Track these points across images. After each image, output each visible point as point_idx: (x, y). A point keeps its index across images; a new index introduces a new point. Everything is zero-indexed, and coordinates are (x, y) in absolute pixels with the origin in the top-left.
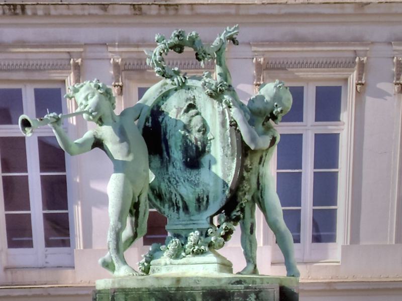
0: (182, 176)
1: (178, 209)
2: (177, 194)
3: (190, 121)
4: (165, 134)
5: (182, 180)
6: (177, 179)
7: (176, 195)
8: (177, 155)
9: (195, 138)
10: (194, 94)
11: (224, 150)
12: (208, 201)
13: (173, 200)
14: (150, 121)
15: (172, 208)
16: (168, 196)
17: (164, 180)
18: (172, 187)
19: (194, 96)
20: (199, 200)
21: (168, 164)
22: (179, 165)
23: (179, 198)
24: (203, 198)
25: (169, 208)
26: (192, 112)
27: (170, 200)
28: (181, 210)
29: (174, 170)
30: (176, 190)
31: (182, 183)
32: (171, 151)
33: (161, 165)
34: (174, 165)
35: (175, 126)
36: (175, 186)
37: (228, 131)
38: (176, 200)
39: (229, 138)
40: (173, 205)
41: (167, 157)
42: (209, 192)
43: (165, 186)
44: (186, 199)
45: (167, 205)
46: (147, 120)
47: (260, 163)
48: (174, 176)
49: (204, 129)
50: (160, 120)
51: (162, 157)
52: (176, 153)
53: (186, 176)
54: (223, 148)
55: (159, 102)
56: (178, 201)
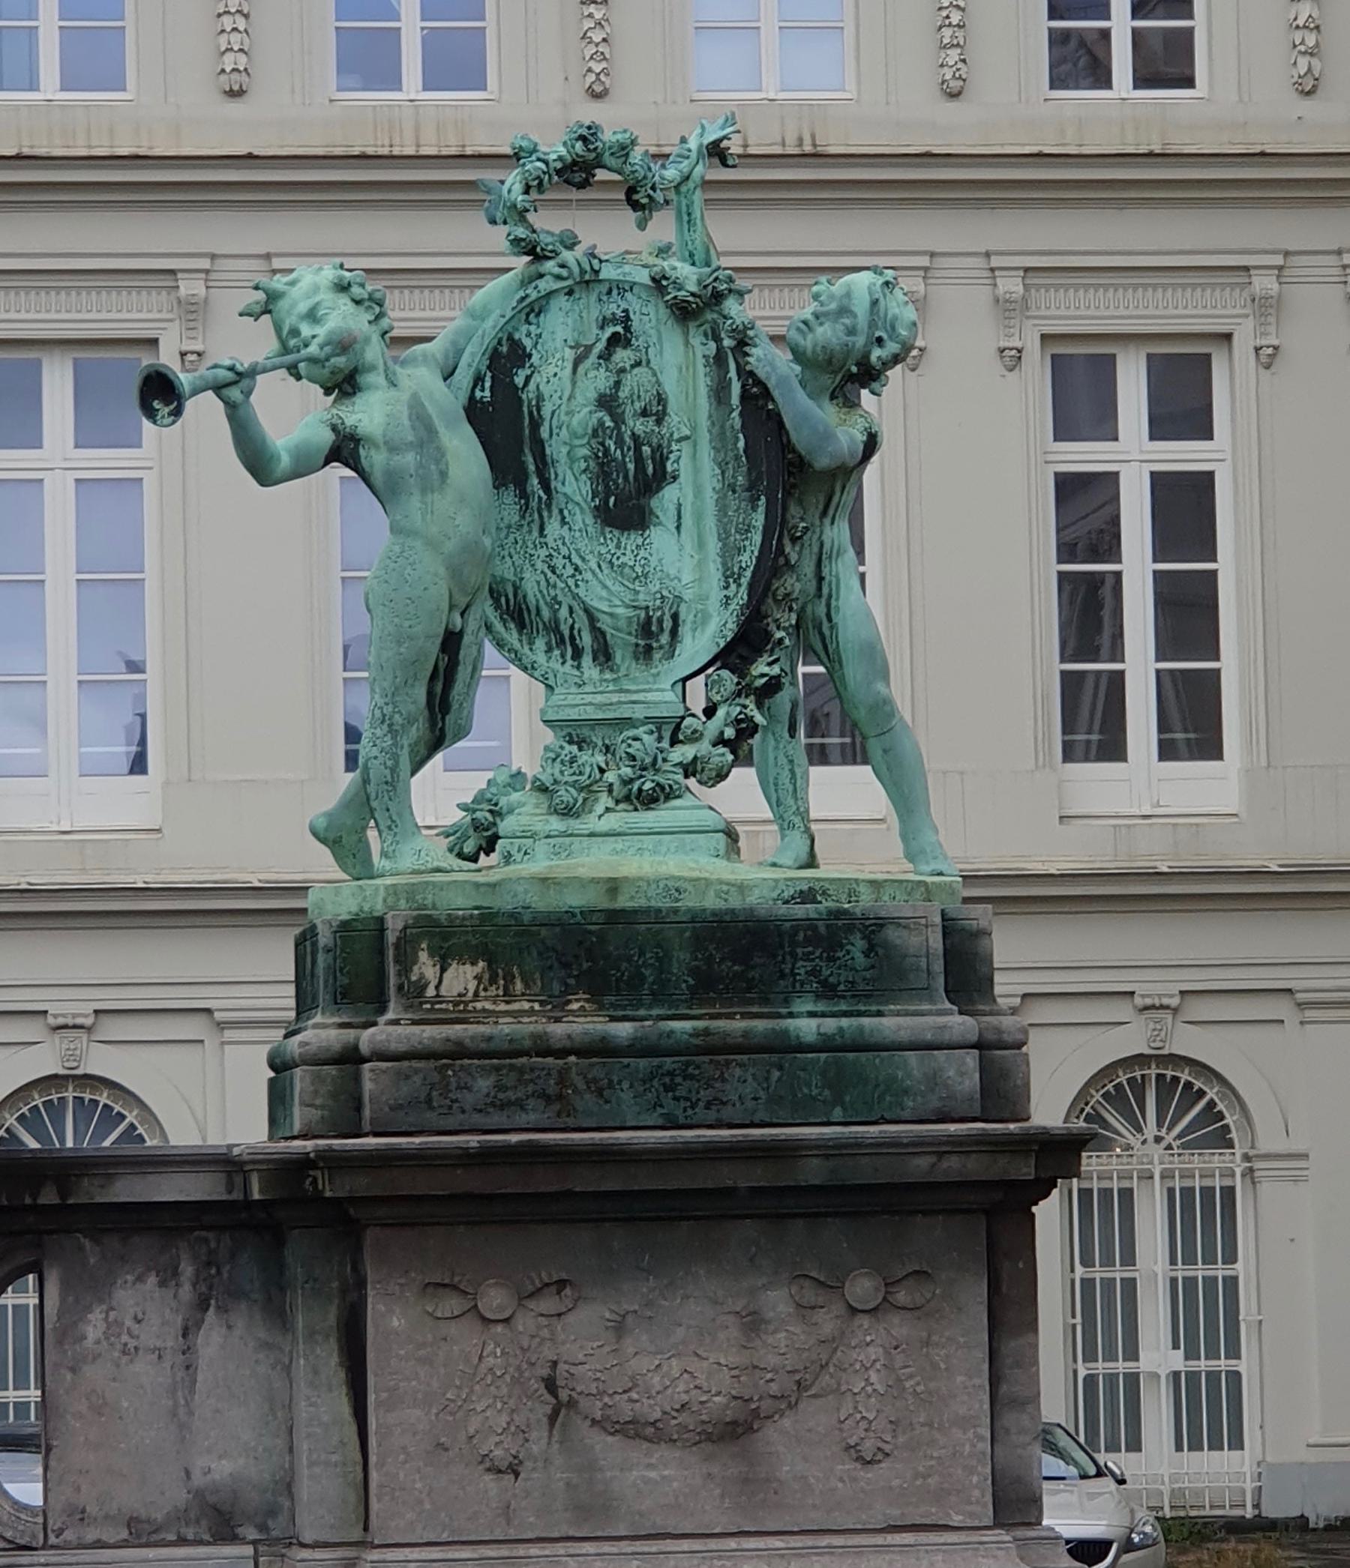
1: (577, 654)
2: (576, 608)
3: (618, 384)
4: (536, 424)
5: (595, 566)
6: (576, 560)
7: (571, 611)
8: (574, 486)
9: (633, 434)
10: (624, 305)
11: (723, 473)
12: (674, 632)
14: (488, 384)
15: (557, 652)
16: (546, 613)
19: (626, 311)
20: (647, 628)
21: (545, 514)
24: (660, 621)
25: (549, 650)
26: (622, 356)
27: (553, 628)
28: (587, 660)
33: (523, 517)
34: (563, 518)
35: (569, 399)
37: (735, 414)
38: (572, 628)
39: (741, 436)
40: (561, 642)
42: (679, 599)
43: (538, 583)
44: (605, 623)
45: (540, 644)
46: (478, 380)
47: (824, 513)
48: (564, 551)
49: (657, 410)
50: (519, 380)
51: (524, 494)
54: (722, 466)
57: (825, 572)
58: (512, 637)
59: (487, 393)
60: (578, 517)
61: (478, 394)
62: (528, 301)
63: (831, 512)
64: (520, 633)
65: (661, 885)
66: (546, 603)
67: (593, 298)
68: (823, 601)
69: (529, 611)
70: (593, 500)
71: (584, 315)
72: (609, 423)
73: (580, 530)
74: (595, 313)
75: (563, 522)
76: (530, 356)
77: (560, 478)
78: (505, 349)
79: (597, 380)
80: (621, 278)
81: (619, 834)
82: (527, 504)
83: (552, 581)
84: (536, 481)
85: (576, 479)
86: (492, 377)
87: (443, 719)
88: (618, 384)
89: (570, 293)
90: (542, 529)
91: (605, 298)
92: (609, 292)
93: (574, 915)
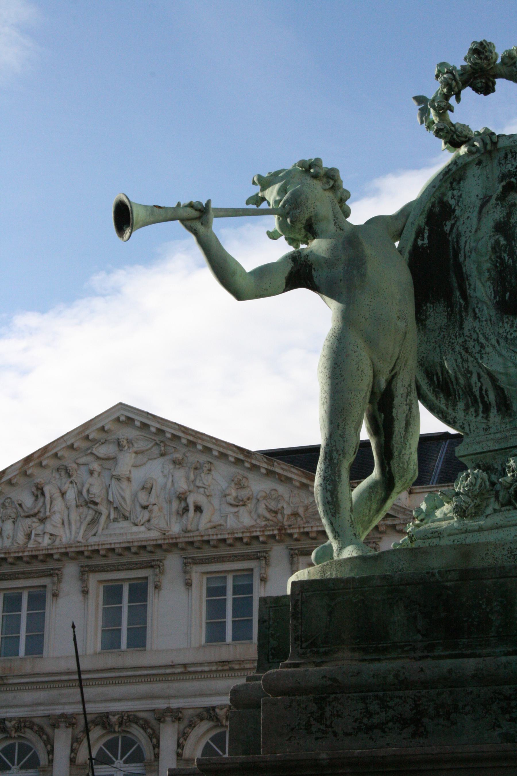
0: (493, 333)
1: (487, 409)
2: (482, 374)
3: (509, 215)
4: (456, 253)
5: (494, 342)
6: (482, 340)
7: (479, 377)
13: (474, 390)
14: (426, 235)
15: (472, 410)
16: (462, 381)
17: (453, 350)
18: (471, 359)
21: (464, 314)
22: (488, 311)
23: (487, 384)
25: (467, 409)
27: (469, 390)
28: (494, 411)
29: (476, 324)
30: (480, 366)
31: (494, 347)
32: (470, 285)
33: (449, 319)
34: (475, 314)
36: (478, 356)
38: (481, 389)
40: (475, 401)
41: (461, 301)
43: (456, 360)
45: (461, 405)
46: (419, 233)
48: (474, 336)
50: (447, 228)
51: (450, 305)
52: (479, 285)
53: (501, 331)
55: (444, 194)
56: (486, 391)
58: (442, 403)
59: (426, 241)
60: (486, 312)
61: (420, 242)
62: (451, 173)
64: (447, 399)
65: (506, 548)
66: (461, 374)
67: (496, 162)
69: (452, 383)
70: (495, 298)
71: (490, 176)
72: (503, 242)
73: (486, 321)
74: (497, 173)
75: (475, 317)
76: (454, 211)
77: (472, 287)
78: (437, 210)
79: (496, 214)
80: (512, 144)
81: (501, 527)
82: (452, 311)
83: (465, 357)
84: (458, 294)
85: (484, 286)
86: (429, 230)
87: (389, 464)
88: (509, 215)
89: (479, 163)
90: (461, 324)
91: (503, 162)
92: (506, 157)
93: (433, 575)
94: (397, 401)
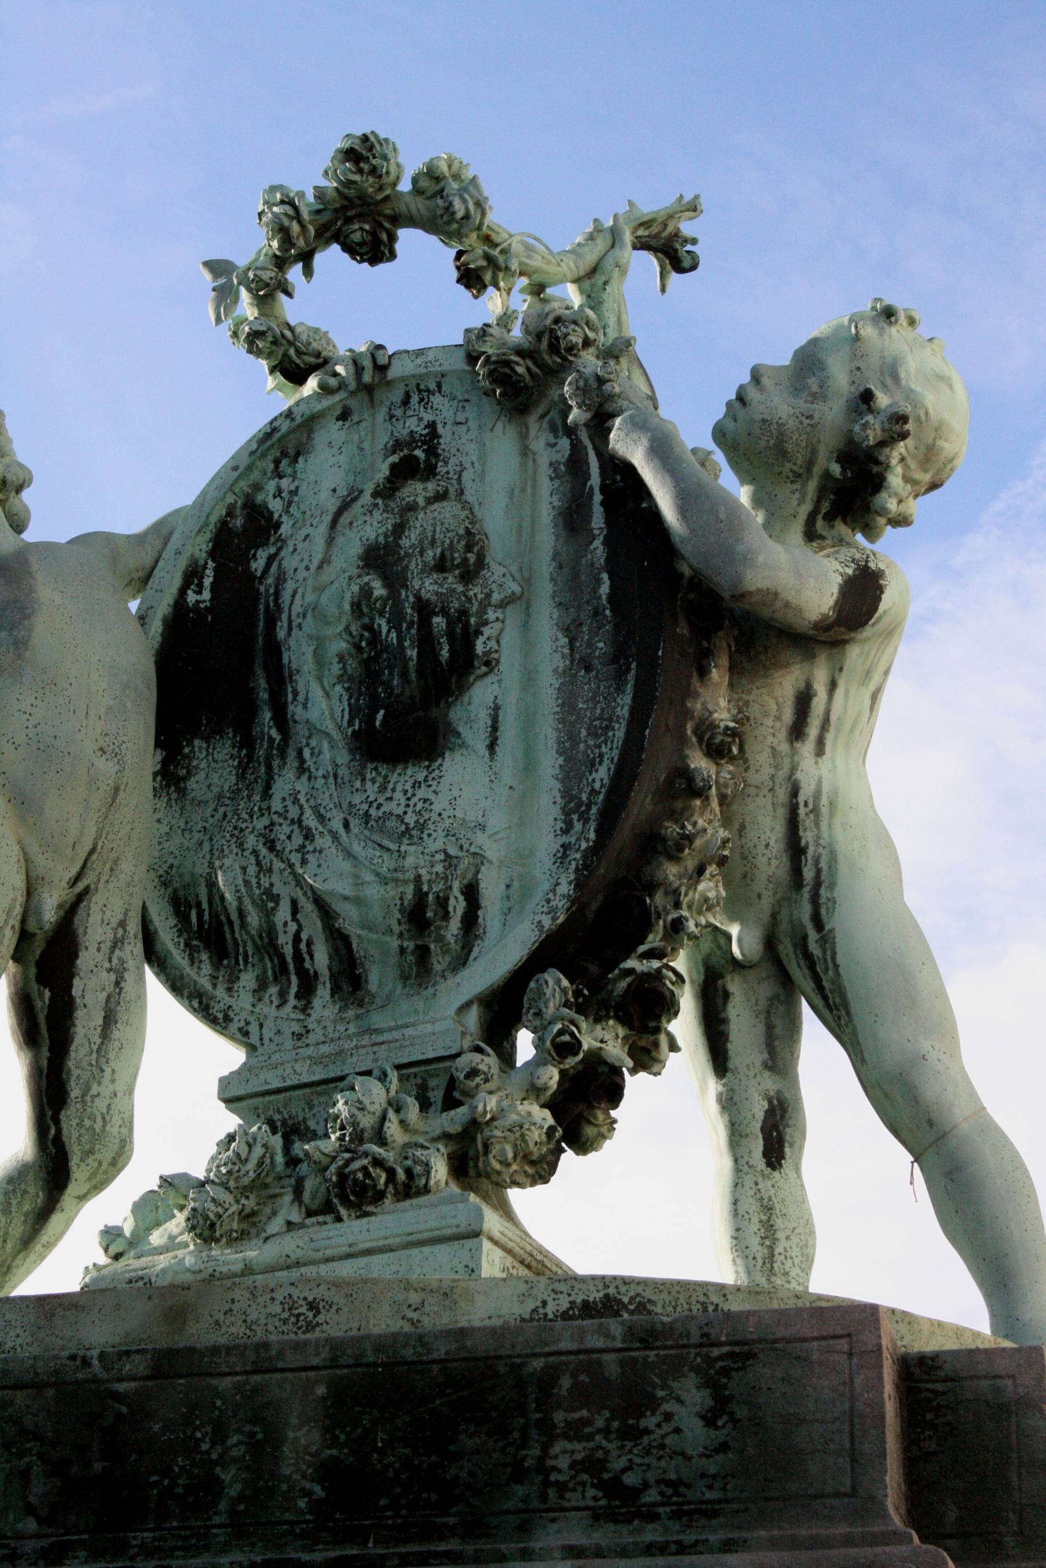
2: (303, 901)
3: (399, 529)
4: (272, 621)
5: (337, 825)
6: (310, 820)
7: (295, 909)
8: (322, 705)
9: (418, 599)
10: (428, 417)
11: (571, 644)
12: (470, 920)
13: (282, 939)
14: (207, 582)
15: (273, 990)
16: (254, 919)
17: (241, 845)
18: (278, 865)
19: (432, 426)
20: (419, 915)
21: (276, 763)
22: (331, 753)
23: (313, 925)
24: (443, 902)
26: (416, 491)
28: (323, 992)
29: (302, 786)
30: (299, 881)
31: (335, 836)
32: (295, 693)
33: (241, 777)
35: (320, 567)
36: (295, 858)
37: (597, 543)
39: (605, 576)
41: (274, 732)
42: (479, 859)
43: (244, 869)
44: (349, 919)
45: (248, 979)
46: (192, 576)
48: (294, 812)
49: (466, 559)
51: (247, 741)
52: (317, 693)
53: (357, 799)
54: (571, 632)
55: (257, 487)
56: (309, 944)
57: (807, 836)
58: (202, 975)
59: (206, 595)
60: (327, 755)
61: (192, 597)
62: (277, 435)
63: (813, 731)
64: (216, 965)
65: (279, 1296)
66: (253, 902)
67: (382, 413)
68: (806, 892)
69: (231, 923)
70: (350, 723)
71: (366, 445)
72: (379, 590)
73: (324, 777)
74: (383, 439)
75: (302, 769)
76: (278, 525)
77: (301, 698)
78: (239, 522)
79: (369, 527)
80: (423, 370)
82: (250, 757)
83: (266, 862)
84: (267, 715)
85: (327, 695)
86: (215, 570)
87: (57, 1121)
88: (399, 529)
89: (344, 415)
90: (268, 786)
91: (398, 412)
92: (406, 402)
93: (86, 1362)
94: (85, 960)
